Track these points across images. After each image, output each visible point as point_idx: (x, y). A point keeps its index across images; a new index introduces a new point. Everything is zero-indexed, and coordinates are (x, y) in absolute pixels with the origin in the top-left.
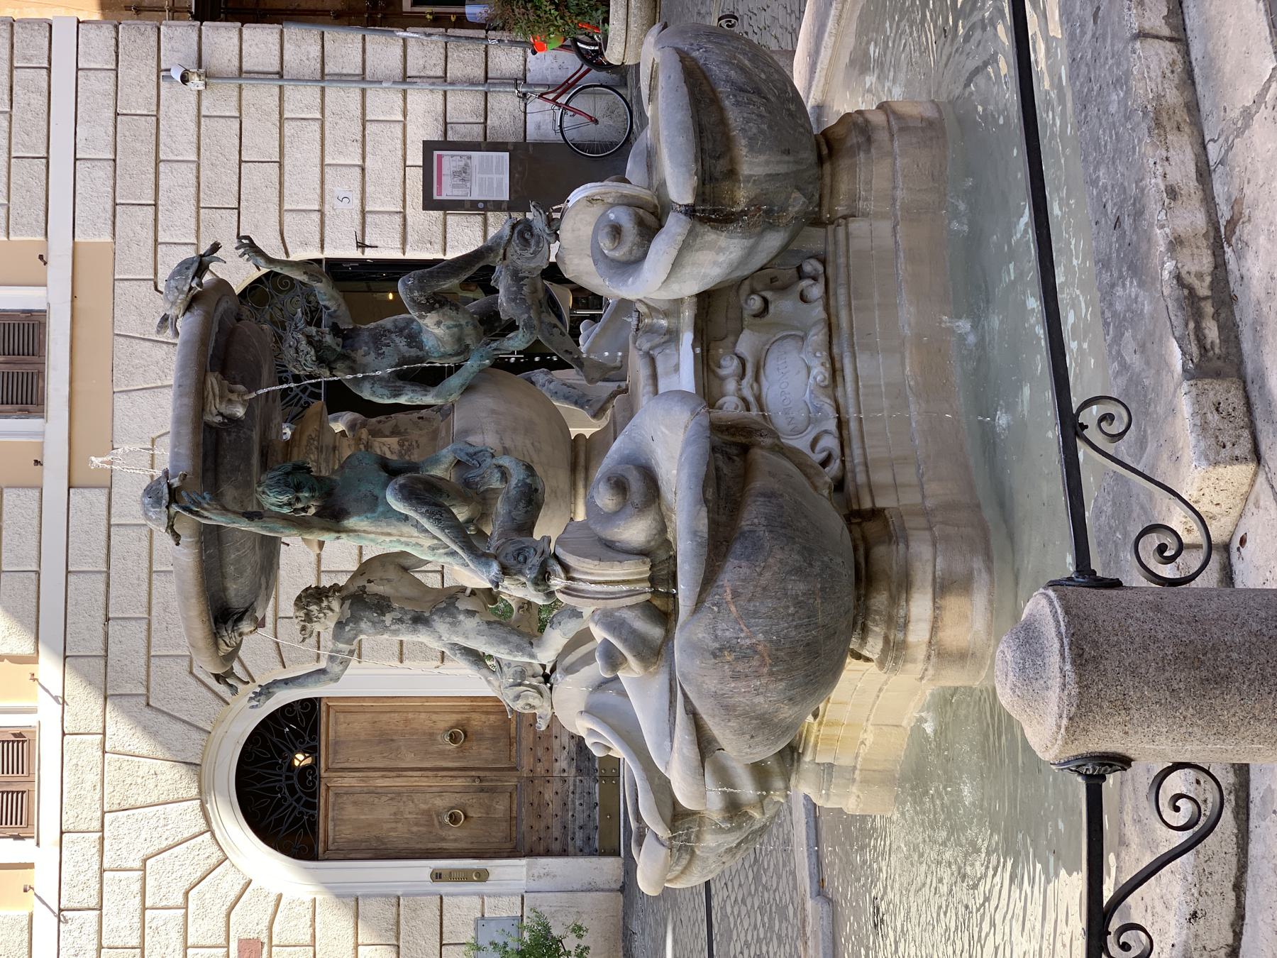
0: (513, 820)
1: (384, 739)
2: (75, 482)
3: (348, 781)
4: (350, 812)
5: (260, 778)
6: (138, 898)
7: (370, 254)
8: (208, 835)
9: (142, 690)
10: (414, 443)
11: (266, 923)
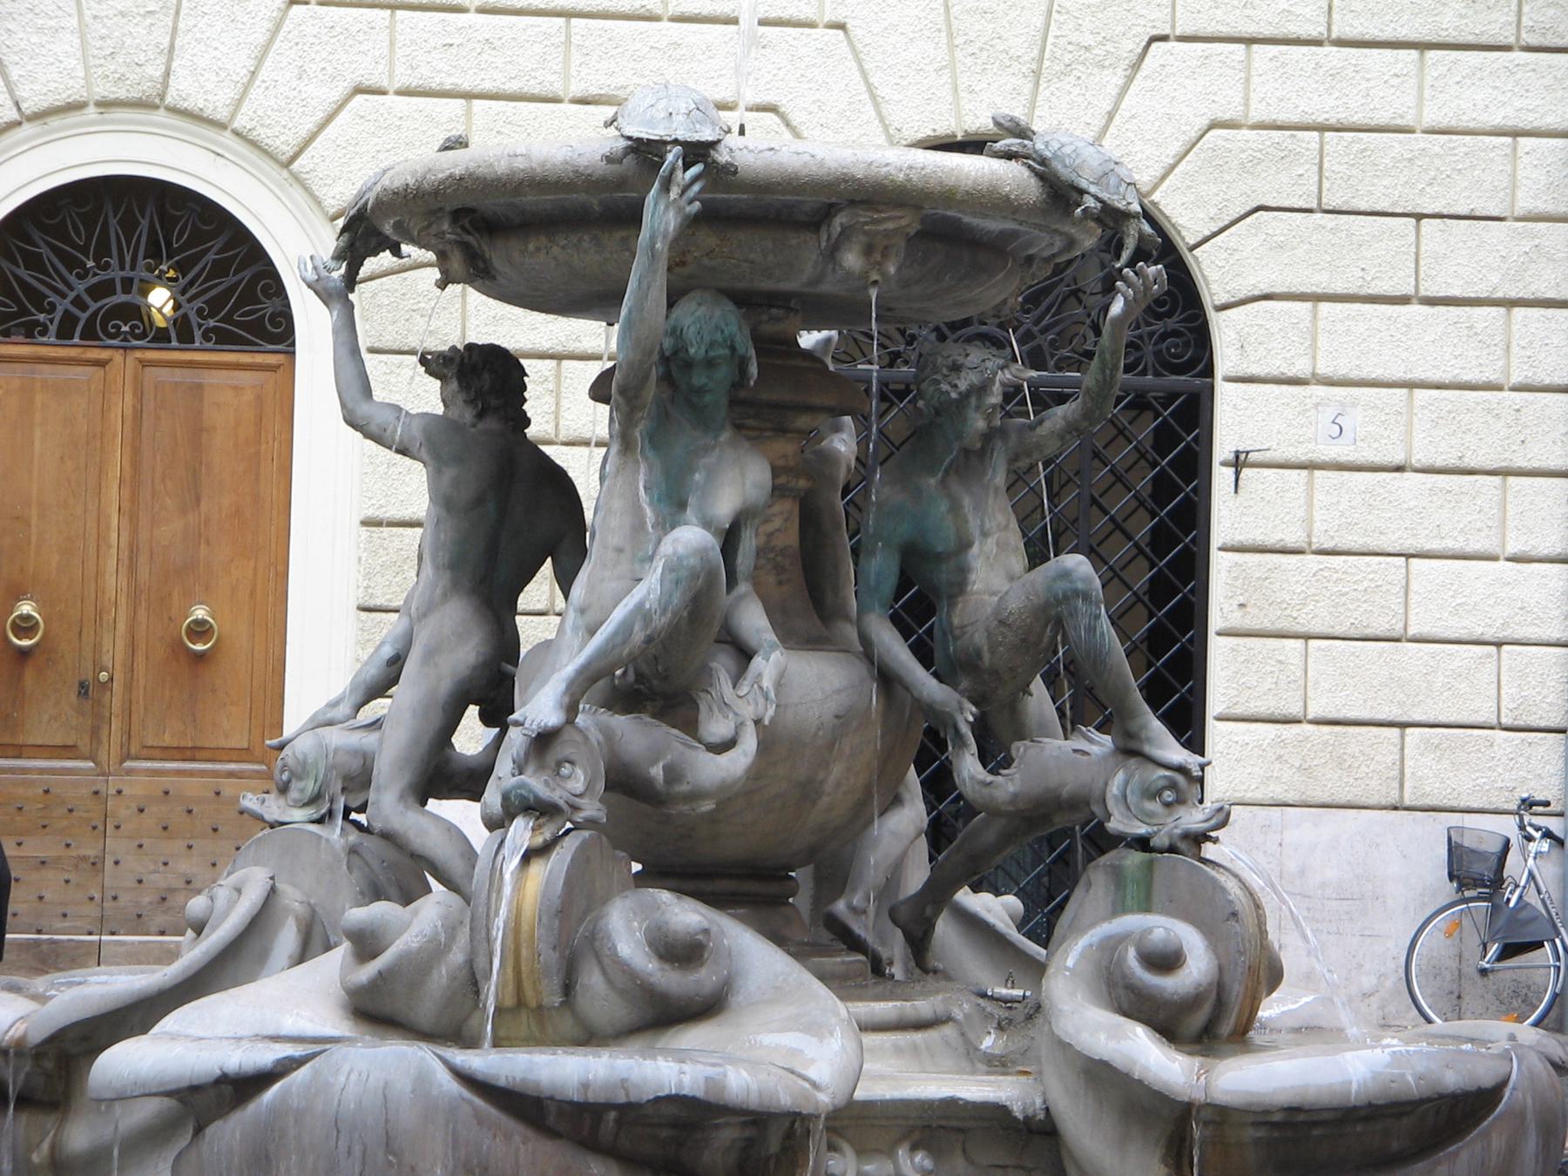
5: (129, 226)
7: (1222, 477)
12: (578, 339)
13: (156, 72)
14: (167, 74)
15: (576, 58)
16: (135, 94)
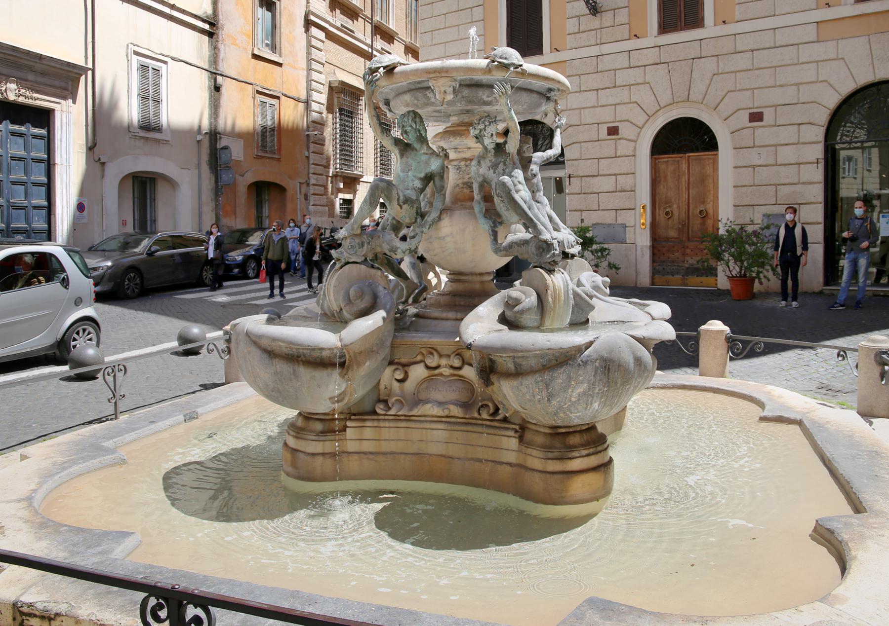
0: (667, 239)
1: (703, 180)
2: (820, 25)
3: (684, 166)
4: (671, 168)
6: (634, 82)
8: (659, 108)
9: (720, 71)
11: (625, 136)
14: (689, 95)
16: (682, 100)
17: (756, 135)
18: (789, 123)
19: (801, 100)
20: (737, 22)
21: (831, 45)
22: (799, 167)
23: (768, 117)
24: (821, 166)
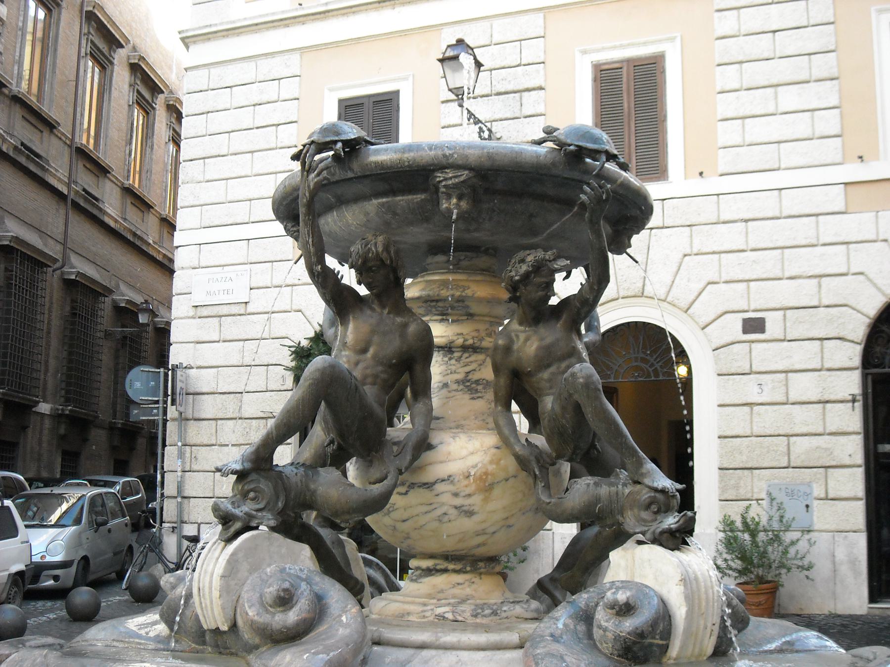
10: (479, 395)
12: (793, 365)
13: (640, 285)
14: (644, 286)
15: (786, 263)
16: (633, 294)
17: (753, 354)
18: (805, 338)
19: (826, 302)
20: (721, 175)
21: (869, 216)
22: (824, 408)
23: (773, 327)
24: (859, 405)
